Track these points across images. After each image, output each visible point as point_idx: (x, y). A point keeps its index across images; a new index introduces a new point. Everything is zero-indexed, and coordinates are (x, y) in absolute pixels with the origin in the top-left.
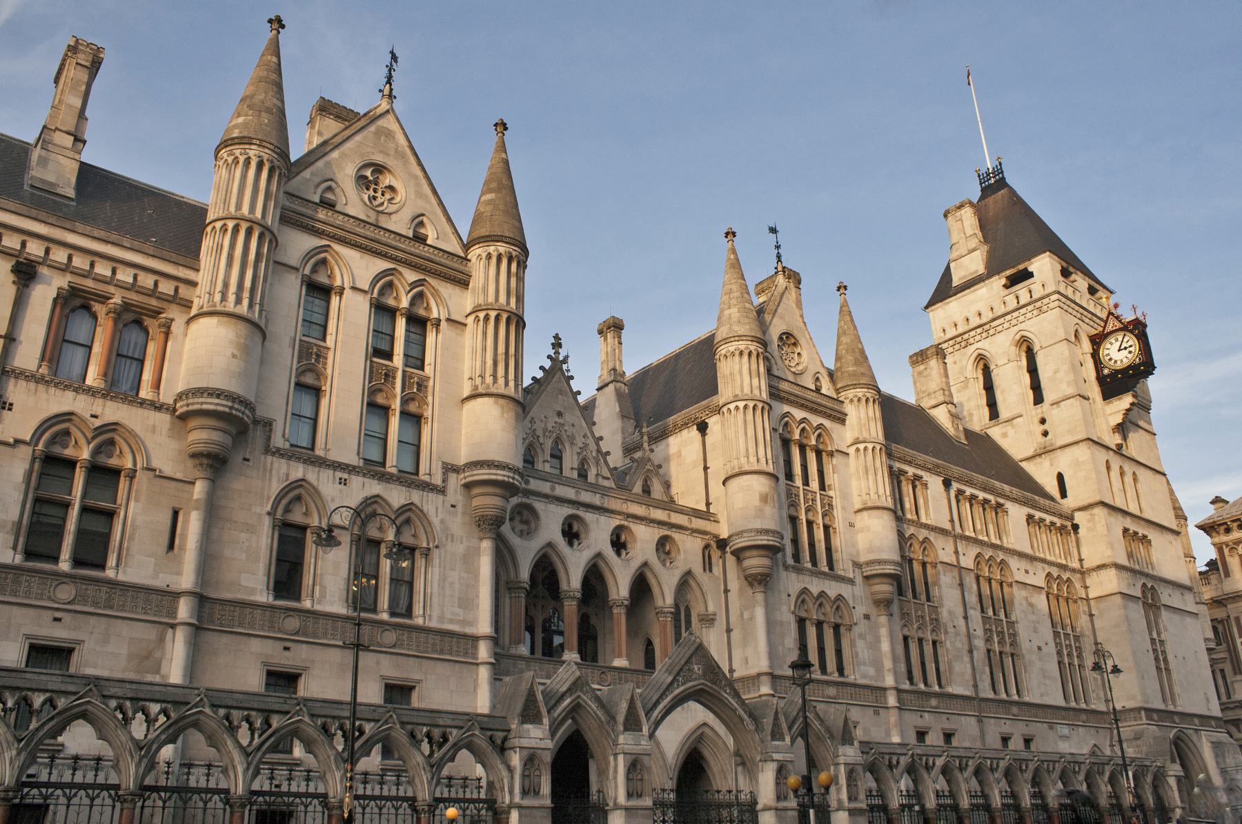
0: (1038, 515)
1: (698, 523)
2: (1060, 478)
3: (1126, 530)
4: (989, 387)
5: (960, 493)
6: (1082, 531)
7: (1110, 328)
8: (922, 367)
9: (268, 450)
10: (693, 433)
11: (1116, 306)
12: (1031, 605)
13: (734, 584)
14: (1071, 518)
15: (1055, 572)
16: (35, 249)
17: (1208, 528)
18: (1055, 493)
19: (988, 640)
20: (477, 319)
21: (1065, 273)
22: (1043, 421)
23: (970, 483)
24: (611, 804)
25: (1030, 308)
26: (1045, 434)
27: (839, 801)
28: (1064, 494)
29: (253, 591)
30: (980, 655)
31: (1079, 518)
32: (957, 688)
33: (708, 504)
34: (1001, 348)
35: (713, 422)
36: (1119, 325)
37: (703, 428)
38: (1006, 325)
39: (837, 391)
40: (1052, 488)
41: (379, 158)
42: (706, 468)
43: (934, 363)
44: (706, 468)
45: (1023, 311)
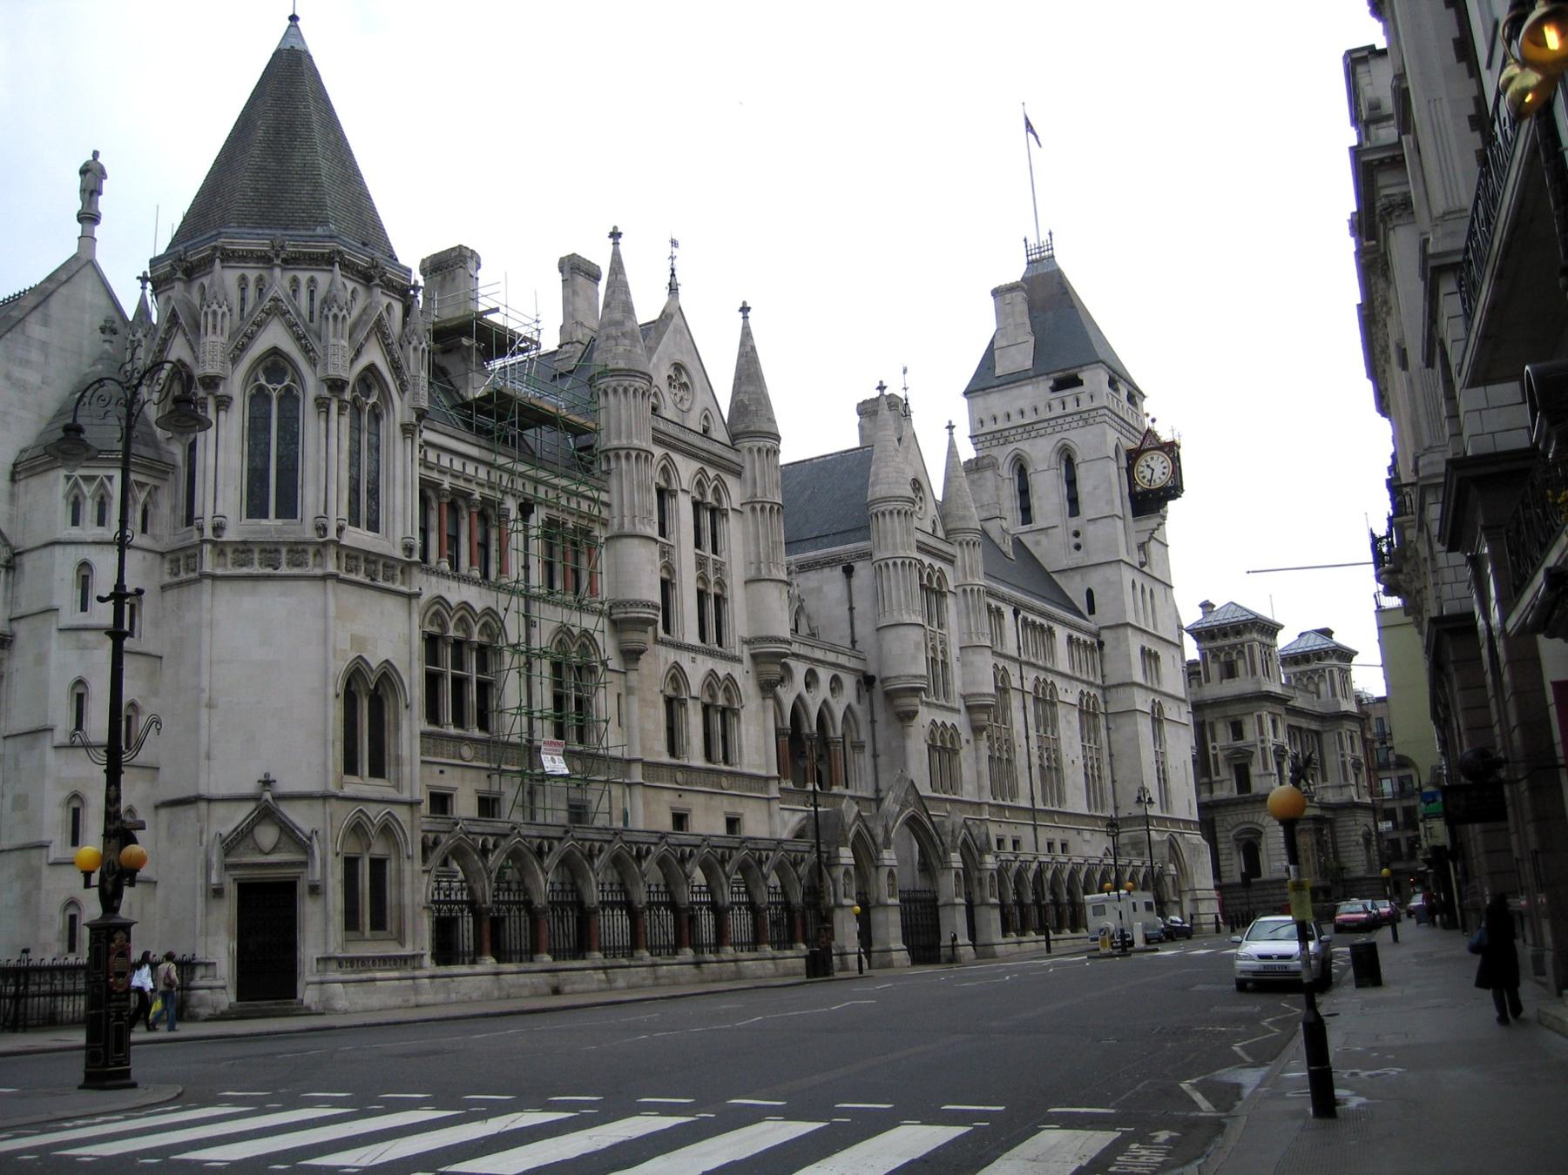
0: (1076, 634)
1: (853, 663)
2: (1090, 594)
3: (1143, 649)
4: (1024, 492)
5: (1025, 619)
6: (1107, 649)
7: (1147, 445)
8: (976, 476)
9: (657, 641)
10: (838, 572)
11: (1153, 420)
12: (1069, 722)
13: (881, 717)
14: (1097, 635)
15: (1086, 689)
16: (529, 490)
17: (1199, 634)
18: (1084, 608)
19: (1041, 757)
20: (753, 509)
21: (1112, 383)
22: (1077, 534)
23: (1031, 609)
24: (873, 903)
25: (1076, 417)
26: (1078, 547)
27: (982, 898)
28: (1092, 610)
29: (659, 753)
30: (1035, 771)
31: (1105, 636)
32: (1024, 802)
33: (853, 642)
34: (1040, 453)
35: (862, 570)
36: (1155, 444)
37: (849, 571)
38: (1049, 430)
39: (948, 533)
40: (1082, 605)
41: (678, 358)
42: (851, 609)
43: (989, 474)
44: (851, 609)
45: (1069, 419)
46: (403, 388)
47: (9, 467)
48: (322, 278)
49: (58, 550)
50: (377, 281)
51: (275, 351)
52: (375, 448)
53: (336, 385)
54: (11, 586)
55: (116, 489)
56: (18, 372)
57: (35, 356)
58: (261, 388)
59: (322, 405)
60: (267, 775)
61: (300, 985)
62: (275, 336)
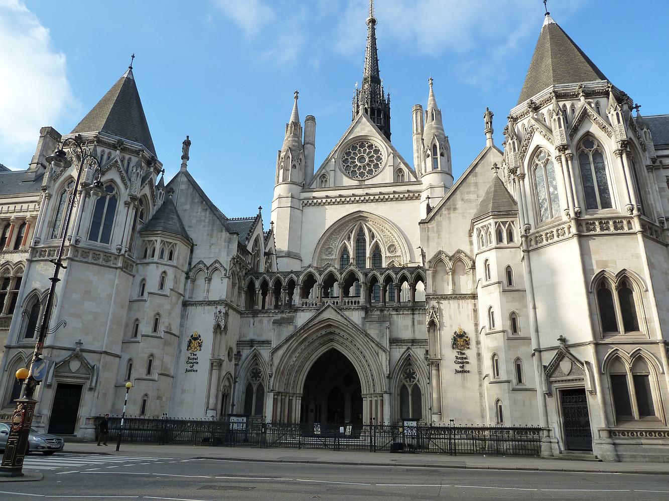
46: (609, 135)
47: (468, 231)
48: (551, 107)
49: (477, 256)
50: (581, 94)
51: (538, 147)
52: (601, 169)
53: (563, 148)
54: (474, 274)
55: (493, 230)
56: (466, 197)
57: (472, 189)
58: (537, 165)
59: (559, 159)
60: (561, 336)
61: (593, 445)
62: (538, 139)
